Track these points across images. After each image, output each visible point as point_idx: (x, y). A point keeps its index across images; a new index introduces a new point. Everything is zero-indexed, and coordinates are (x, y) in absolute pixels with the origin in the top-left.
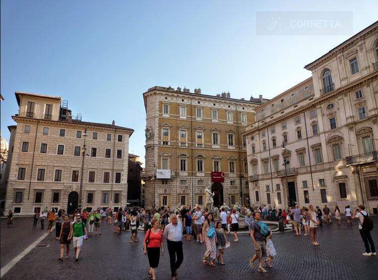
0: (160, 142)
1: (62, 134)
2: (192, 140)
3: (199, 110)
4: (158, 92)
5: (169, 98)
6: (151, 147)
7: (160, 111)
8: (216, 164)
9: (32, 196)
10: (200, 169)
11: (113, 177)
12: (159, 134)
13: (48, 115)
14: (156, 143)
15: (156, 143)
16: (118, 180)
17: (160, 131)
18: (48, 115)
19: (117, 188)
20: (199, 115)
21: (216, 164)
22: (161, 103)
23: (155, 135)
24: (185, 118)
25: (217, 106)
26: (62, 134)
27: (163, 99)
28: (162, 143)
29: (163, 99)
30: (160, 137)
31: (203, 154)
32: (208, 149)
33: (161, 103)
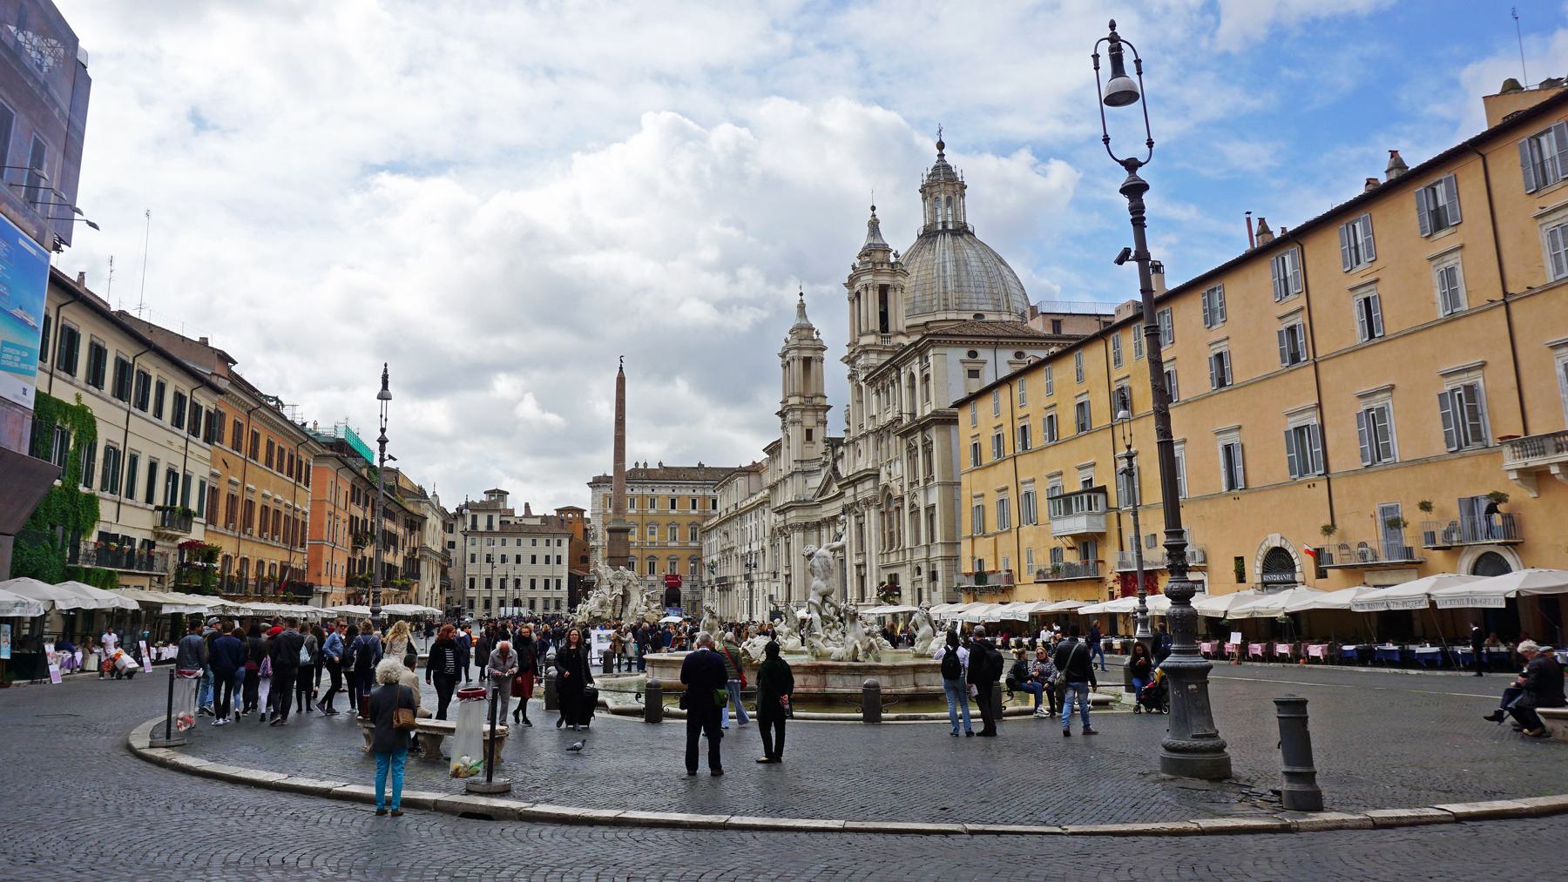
2: (642, 537)
3: (652, 502)
8: (673, 564)
9: (482, 604)
10: (652, 571)
11: (553, 584)
13: (490, 526)
16: (558, 587)
18: (490, 526)
19: (558, 595)
20: (653, 506)
21: (673, 564)
22: (605, 496)
25: (677, 492)
31: (655, 553)
32: (664, 547)
33: (605, 496)
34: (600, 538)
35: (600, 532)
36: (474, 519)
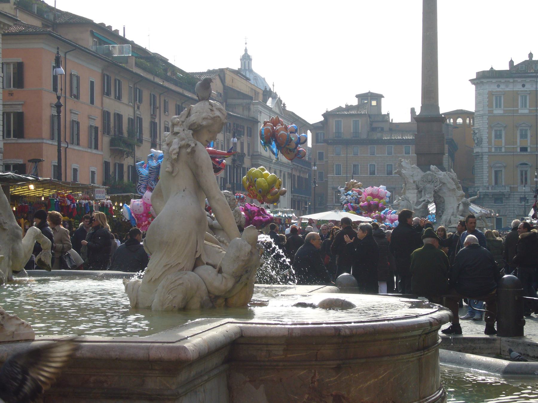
0: (490, 149)
1: (373, 153)
4: (485, 81)
5: (502, 86)
6: (479, 155)
7: (490, 105)
12: (489, 138)
14: (486, 150)
15: (486, 150)
17: (489, 133)
22: (491, 94)
23: (484, 140)
24: (526, 111)
26: (373, 153)
27: (494, 88)
28: (493, 150)
29: (494, 88)
30: (490, 142)
33: (491, 94)
34: (485, 144)
35: (485, 136)
36: (338, 124)
